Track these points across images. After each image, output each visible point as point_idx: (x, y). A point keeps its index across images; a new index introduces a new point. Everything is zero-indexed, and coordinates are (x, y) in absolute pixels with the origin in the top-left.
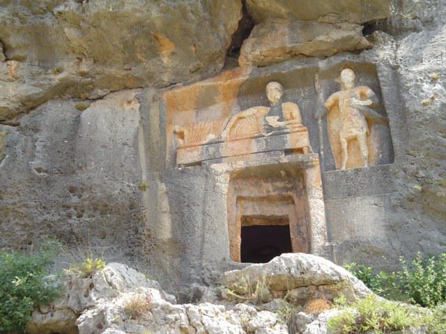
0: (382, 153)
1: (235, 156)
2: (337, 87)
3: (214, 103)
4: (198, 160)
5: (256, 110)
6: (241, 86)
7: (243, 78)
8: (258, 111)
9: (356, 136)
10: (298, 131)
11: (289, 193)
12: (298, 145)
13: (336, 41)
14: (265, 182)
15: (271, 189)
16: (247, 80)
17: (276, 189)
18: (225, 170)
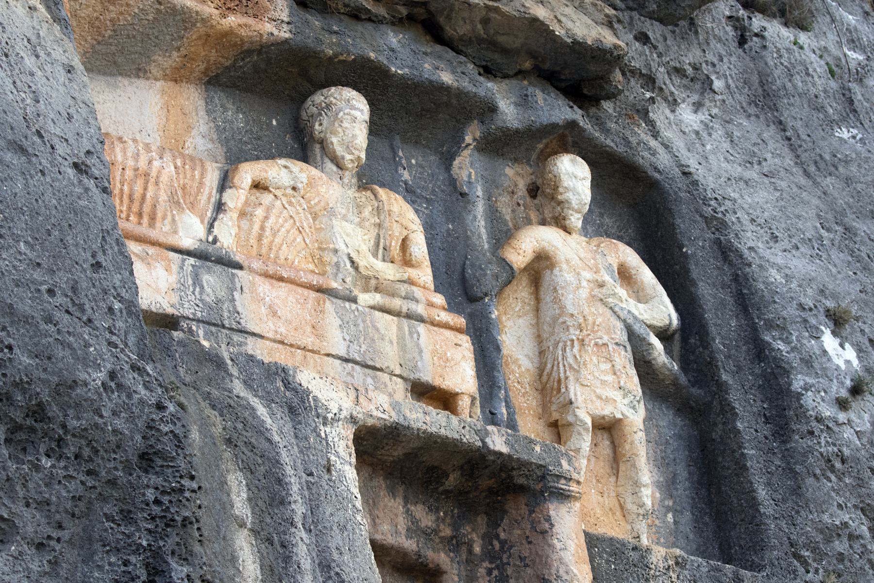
0: (675, 512)
1: (282, 342)
2: (544, 200)
3: (140, 72)
4: (170, 311)
5: (303, 177)
6: (249, 52)
7: (276, 32)
8: (311, 184)
9: (620, 420)
10: (446, 326)
11: (442, 558)
12: (449, 383)
13: (575, 42)
14: (387, 487)
15: (402, 523)
16: (286, 41)
17: (415, 530)
18: (345, 414)
